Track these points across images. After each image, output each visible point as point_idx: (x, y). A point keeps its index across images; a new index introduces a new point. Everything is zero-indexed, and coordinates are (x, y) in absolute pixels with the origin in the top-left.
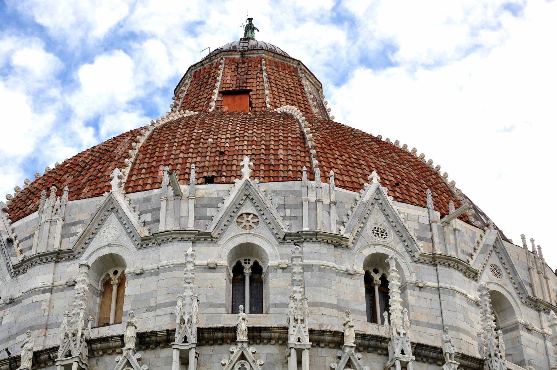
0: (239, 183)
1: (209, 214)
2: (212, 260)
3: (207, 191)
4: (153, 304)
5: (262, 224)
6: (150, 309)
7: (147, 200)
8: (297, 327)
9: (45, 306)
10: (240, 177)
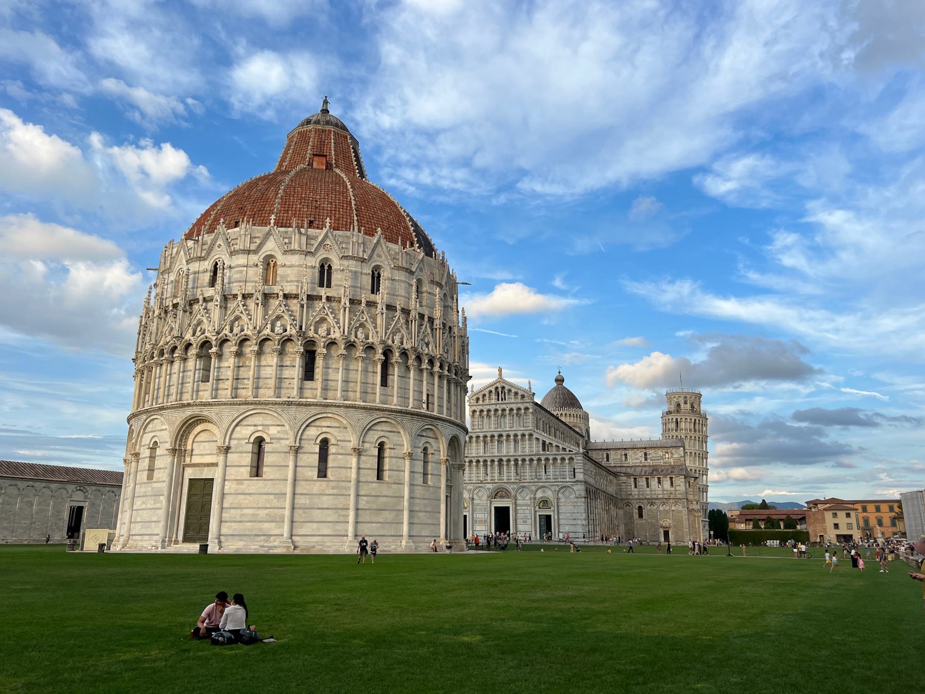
0: (325, 230)
6: (287, 282)
7: (286, 232)
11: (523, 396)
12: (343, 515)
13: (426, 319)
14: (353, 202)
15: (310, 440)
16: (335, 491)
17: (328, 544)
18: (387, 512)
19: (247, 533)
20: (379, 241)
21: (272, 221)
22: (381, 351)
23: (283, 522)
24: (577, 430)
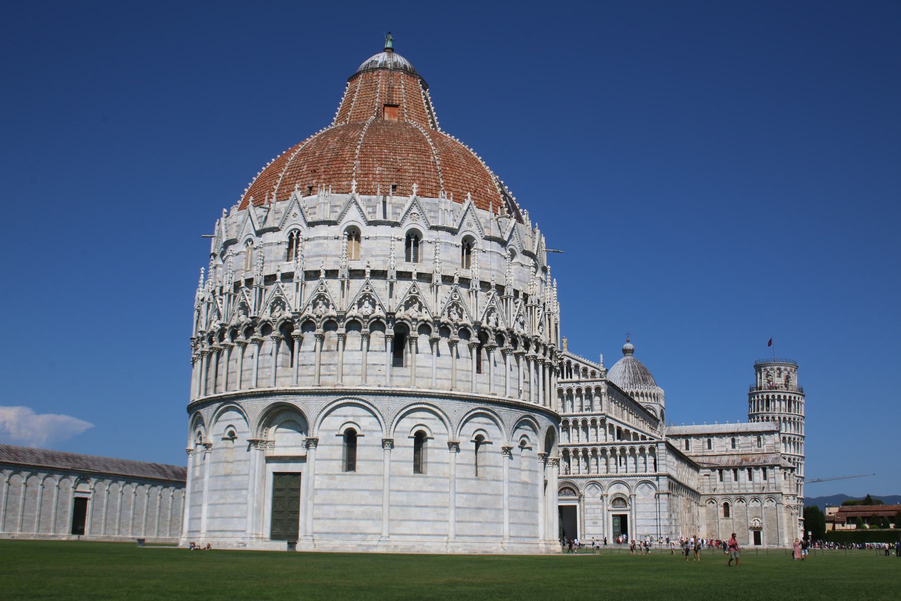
0: (412, 197)
2: (400, 236)
6: (373, 256)
7: (370, 200)
11: (593, 373)
12: (442, 514)
13: (521, 296)
14: (438, 163)
15: (404, 432)
16: (432, 488)
17: (429, 544)
18: (487, 511)
19: (343, 531)
21: (354, 188)
23: (381, 520)
24: (651, 412)
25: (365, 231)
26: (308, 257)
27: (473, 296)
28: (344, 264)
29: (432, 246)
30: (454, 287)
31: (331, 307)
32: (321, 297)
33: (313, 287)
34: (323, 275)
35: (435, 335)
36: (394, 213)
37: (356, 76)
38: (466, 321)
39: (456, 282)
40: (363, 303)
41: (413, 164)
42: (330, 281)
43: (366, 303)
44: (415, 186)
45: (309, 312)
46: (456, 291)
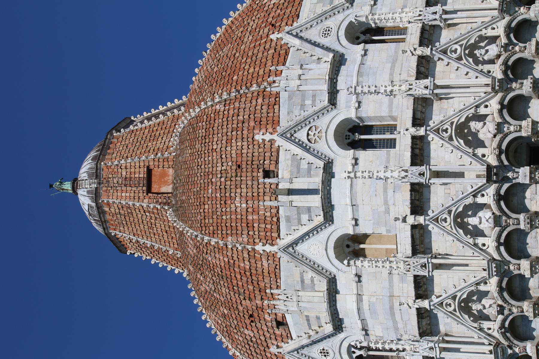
0: (280, 142)
1: (306, 166)
2: (349, 162)
3: (285, 169)
4: (383, 209)
5: (318, 123)
6: (387, 211)
7: (288, 219)
8: (416, 88)
9: (374, 299)
10: (272, 141)
14: (225, 96)
20: (297, 36)
21: (268, 248)
22: (522, 10)
25: (343, 226)
26: (396, 329)
27: (456, 19)
28: (401, 265)
29: (365, 99)
30: (437, 56)
31: (482, 288)
32: (465, 306)
33: (449, 320)
34: (425, 304)
35: (525, 87)
36: (309, 173)
37: (116, 242)
38: (500, 30)
39: (427, 51)
40: (475, 227)
41: (229, 141)
42: (437, 290)
43: (473, 221)
44: (259, 137)
45: (493, 327)
46: (445, 52)
